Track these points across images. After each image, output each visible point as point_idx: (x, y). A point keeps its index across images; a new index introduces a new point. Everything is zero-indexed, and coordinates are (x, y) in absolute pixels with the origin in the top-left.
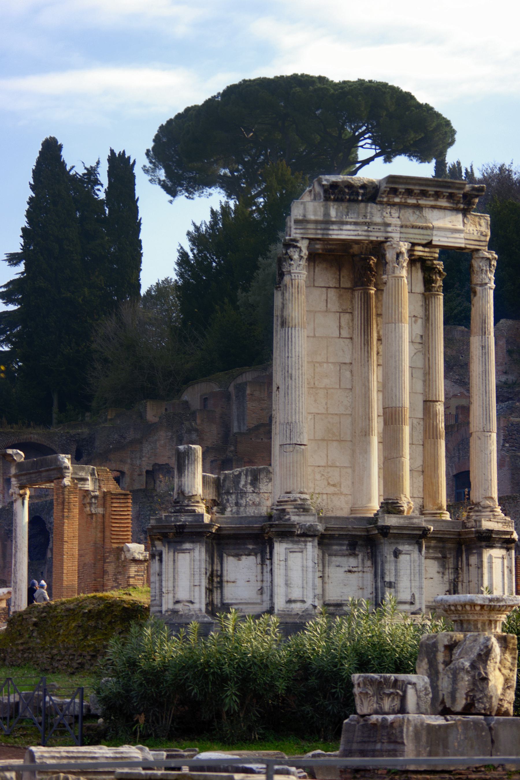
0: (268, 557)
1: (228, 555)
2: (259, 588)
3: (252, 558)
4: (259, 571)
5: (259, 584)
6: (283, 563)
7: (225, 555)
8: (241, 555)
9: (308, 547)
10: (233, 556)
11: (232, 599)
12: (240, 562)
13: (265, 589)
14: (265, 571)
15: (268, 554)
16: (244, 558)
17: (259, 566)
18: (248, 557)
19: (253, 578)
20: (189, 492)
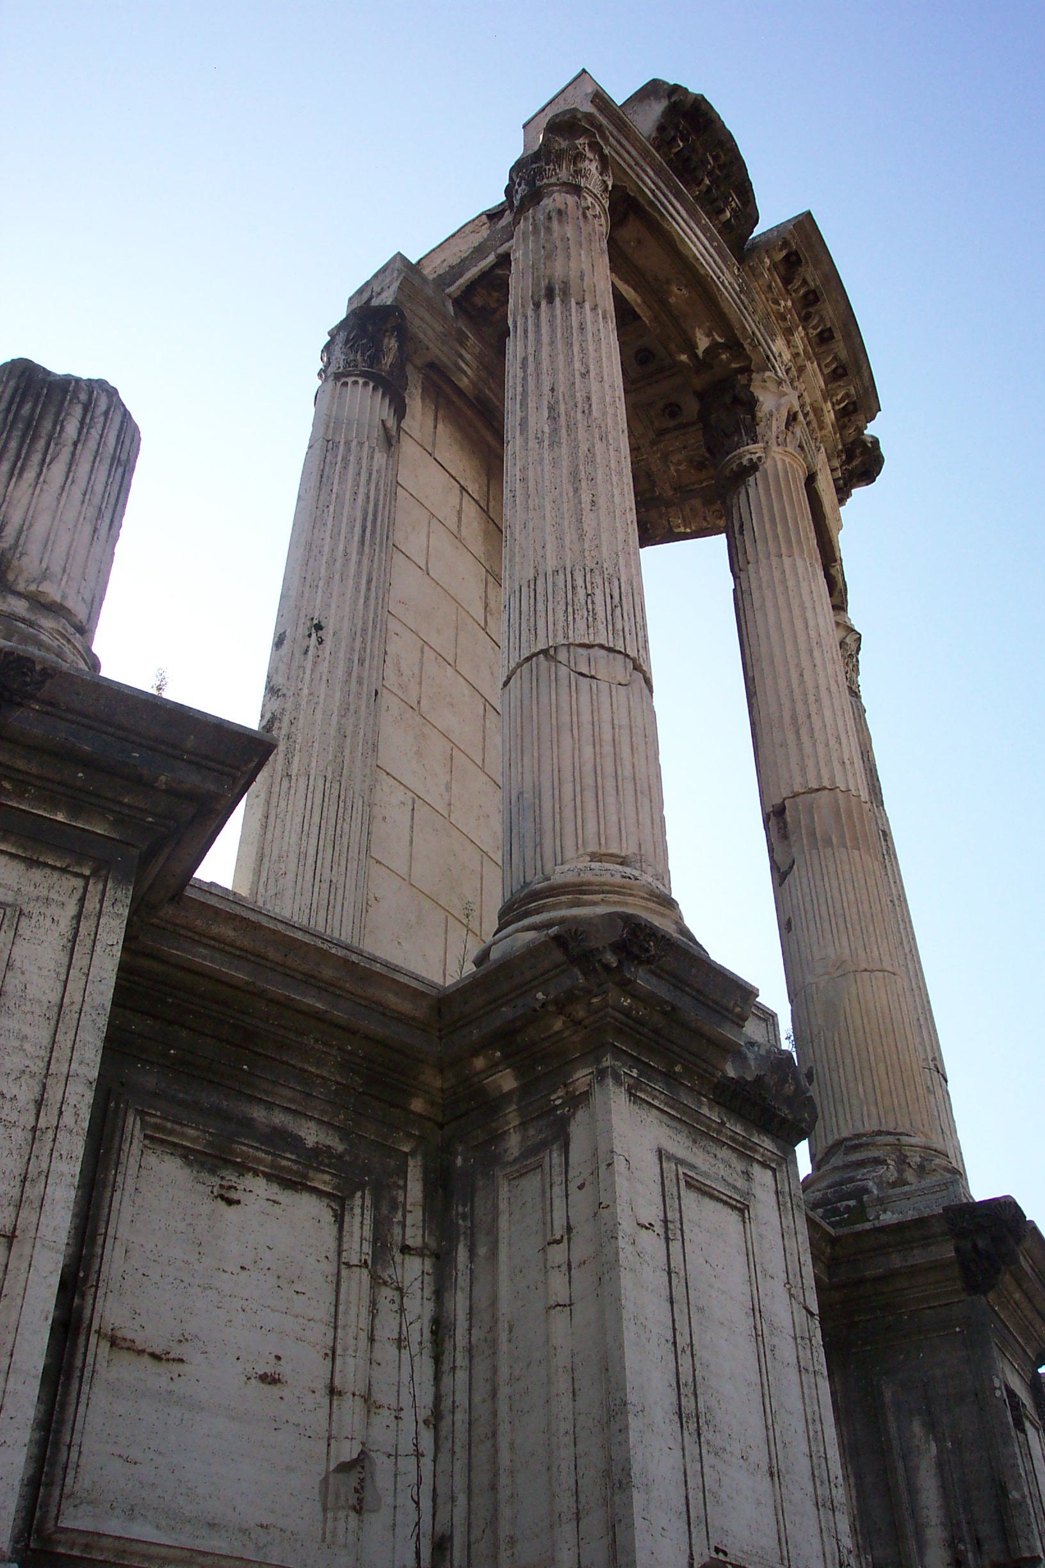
0: (414, 1237)
1: (156, 1141)
2: (348, 1451)
3: (308, 1212)
4: (355, 1315)
5: (350, 1410)
6: (651, 1242)
7: (133, 1124)
8: (243, 1169)
9: (758, 1191)
10: (188, 1156)
11: (131, 1513)
12: (231, 1212)
13: (382, 1466)
14: (388, 1325)
15: (415, 1217)
16: (257, 1190)
17: (357, 1283)
18: (286, 1197)
19: (306, 1368)
20: (45, 576)
